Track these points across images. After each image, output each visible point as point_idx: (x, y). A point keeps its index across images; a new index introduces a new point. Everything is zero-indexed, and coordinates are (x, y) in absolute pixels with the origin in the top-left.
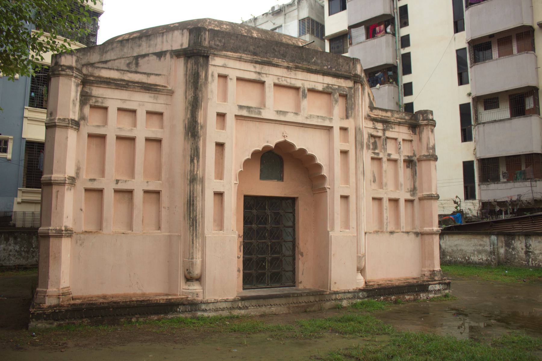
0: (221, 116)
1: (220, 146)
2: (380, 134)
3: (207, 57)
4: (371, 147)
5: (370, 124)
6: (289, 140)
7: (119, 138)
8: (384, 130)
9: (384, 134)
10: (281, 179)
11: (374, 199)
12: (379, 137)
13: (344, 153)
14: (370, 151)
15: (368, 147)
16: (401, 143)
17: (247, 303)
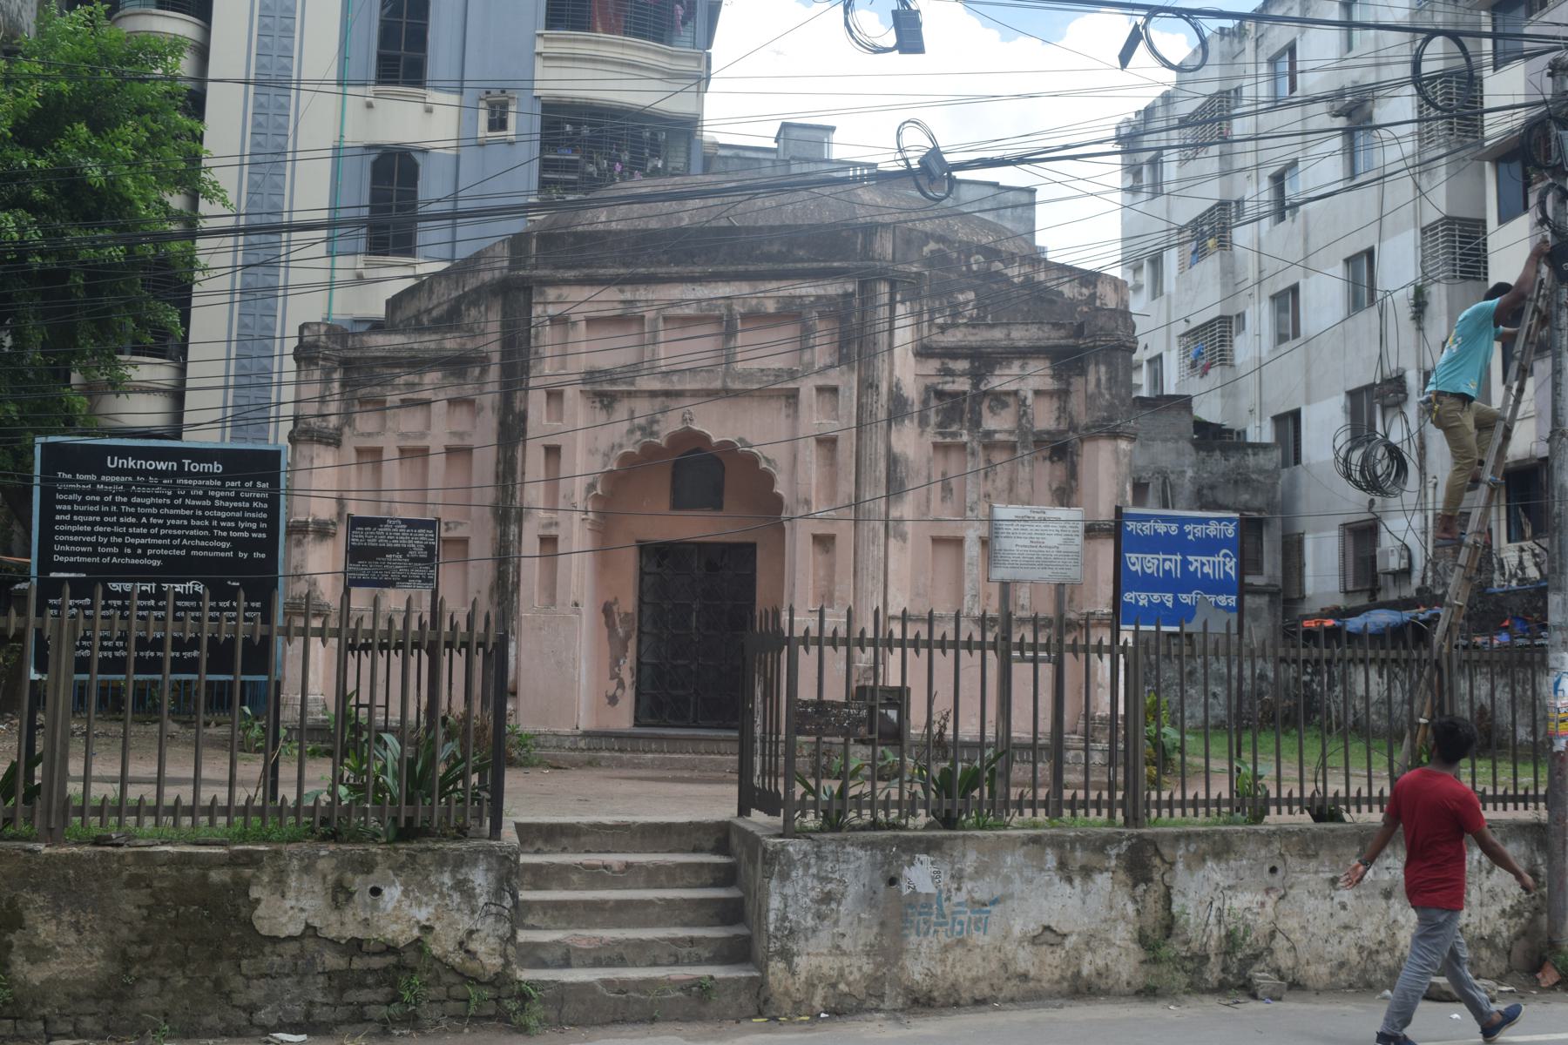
0: (554, 395)
1: (553, 452)
2: (963, 384)
3: (528, 290)
4: (933, 419)
5: (933, 365)
6: (696, 427)
7: (403, 451)
8: (977, 376)
9: (975, 385)
10: (718, 505)
11: (937, 541)
12: (964, 393)
13: (827, 443)
14: (930, 430)
15: (923, 422)
16: (1029, 402)
17: (595, 742)
